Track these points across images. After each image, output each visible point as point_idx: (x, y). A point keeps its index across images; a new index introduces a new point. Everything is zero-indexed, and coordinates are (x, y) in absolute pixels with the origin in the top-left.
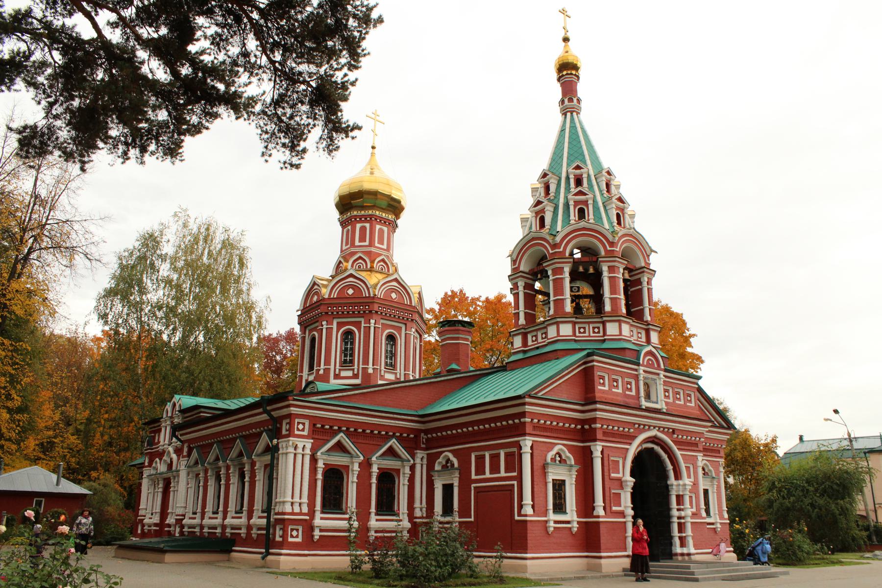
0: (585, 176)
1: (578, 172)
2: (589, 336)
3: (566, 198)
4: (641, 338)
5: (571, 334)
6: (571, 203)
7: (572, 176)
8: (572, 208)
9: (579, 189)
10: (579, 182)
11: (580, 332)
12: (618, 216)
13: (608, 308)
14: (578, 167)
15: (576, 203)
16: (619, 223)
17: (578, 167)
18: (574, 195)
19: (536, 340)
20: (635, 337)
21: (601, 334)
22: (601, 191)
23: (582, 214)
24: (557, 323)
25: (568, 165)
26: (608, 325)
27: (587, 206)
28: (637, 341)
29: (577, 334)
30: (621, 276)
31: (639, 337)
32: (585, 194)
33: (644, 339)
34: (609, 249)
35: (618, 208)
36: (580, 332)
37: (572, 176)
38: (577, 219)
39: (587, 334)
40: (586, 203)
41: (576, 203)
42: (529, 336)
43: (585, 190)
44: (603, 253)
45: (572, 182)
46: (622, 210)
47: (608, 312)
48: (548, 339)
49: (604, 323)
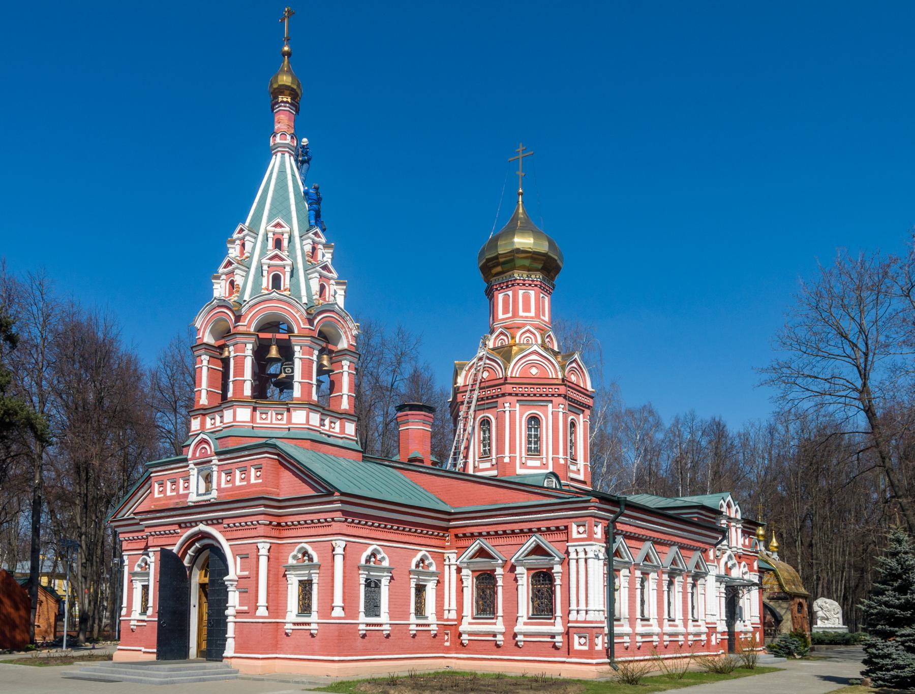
1: (278, 230)
2: (271, 423)
3: (259, 260)
4: (334, 428)
5: (249, 420)
6: (265, 267)
7: (270, 235)
9: (277, 252)
10: (278, 244)
11: (261, 418)
14: (278, 225)
17: (278, 225)
18: (271, 259)
19: (214, 423)
20: (327, 427)
21: (284, 422)
27: (284, 275)
28: (329, 431)
29: (258, 421)
30: (315, 358)
31: (330, 427)
32: (282, 259)
33: (337, 429)
34: (302, 326)
36: (261, 418)
37: (270, 235)
38: (270, 288)
39: (269, 421)
43: (284, 254)
44: (296, 331)
45: (271, 243)
47: (297, 399)
48: (224, 424)
49: (288, 410)
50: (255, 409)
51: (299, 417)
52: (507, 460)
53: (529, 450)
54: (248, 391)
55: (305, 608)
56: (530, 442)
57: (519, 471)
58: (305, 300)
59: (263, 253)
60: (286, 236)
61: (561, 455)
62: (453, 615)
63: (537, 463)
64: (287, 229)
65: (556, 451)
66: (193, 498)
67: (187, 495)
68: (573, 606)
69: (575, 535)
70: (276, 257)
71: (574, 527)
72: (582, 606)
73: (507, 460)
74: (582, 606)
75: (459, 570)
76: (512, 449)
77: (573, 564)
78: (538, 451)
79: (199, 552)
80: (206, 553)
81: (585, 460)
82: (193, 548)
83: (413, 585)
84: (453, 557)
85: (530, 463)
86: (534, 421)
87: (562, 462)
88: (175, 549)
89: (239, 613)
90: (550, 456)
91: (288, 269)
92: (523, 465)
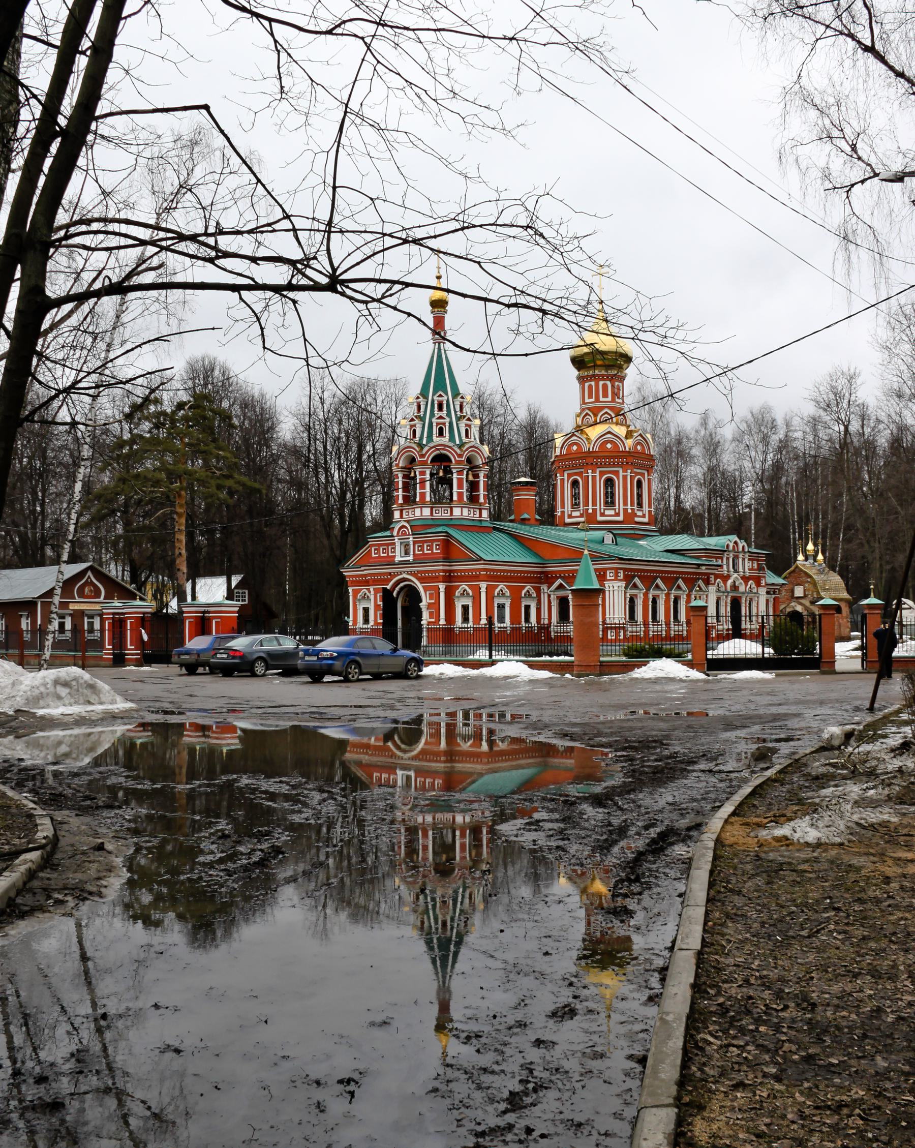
0: (445, 402)
6: (434, 424)
7: (436, 402)
8: (434, 428)
10: (440, 408)
12: (467, 431)
13: (455, 498)
15: (438, 424)
16: (467, 436)
17: (440, 396)
22: (455, 412)
23: (441, 433)
24: (421, 508)
25: (433, 395)
26: (454, 509)
30: (464, 477)
35: (466, 425)
37: (436, 402)
40: (444, 424)
41: (438, 424)
42: (404, 512)
44: (453, 461)
46: (469, 426)
49: (451, 508)
50: (432, 508)
51: (457, 512)
52: (590, 511)
53: (606, 503)
54: (428, 499)
55: (466, 619)
56: (607, 497)
57: (600, 518)
58: (458, 442)
59: (432, 415)
60: (445, 402)
61: (629, 506)
62: (546, 622)
63: (612, 512)
64: (445, 398)
65: (625, 504)
66: (398, 559)
67: (394, 557)
68: (607, 616)
69: (608, 578)
70: (441, 417)
71: (608, 572)
72: (612, 616)
73: (590, 511)
74: (612, 616)
75: (549, 596)
76: (594, 504)
77: (607, 593)
78: (613, 503)
79: (402, 589)
80: (405, 590)
81: (650, 506)
82: (399, 587)
83: (523, 605)
84: (546, 588)
85: (607, 512)
86: (609, 483)
87: (630, 511)
88: (388, 587)
89: (429, 623)
90: (622, 507)
91: (447, 424)
92: (602, 515)
